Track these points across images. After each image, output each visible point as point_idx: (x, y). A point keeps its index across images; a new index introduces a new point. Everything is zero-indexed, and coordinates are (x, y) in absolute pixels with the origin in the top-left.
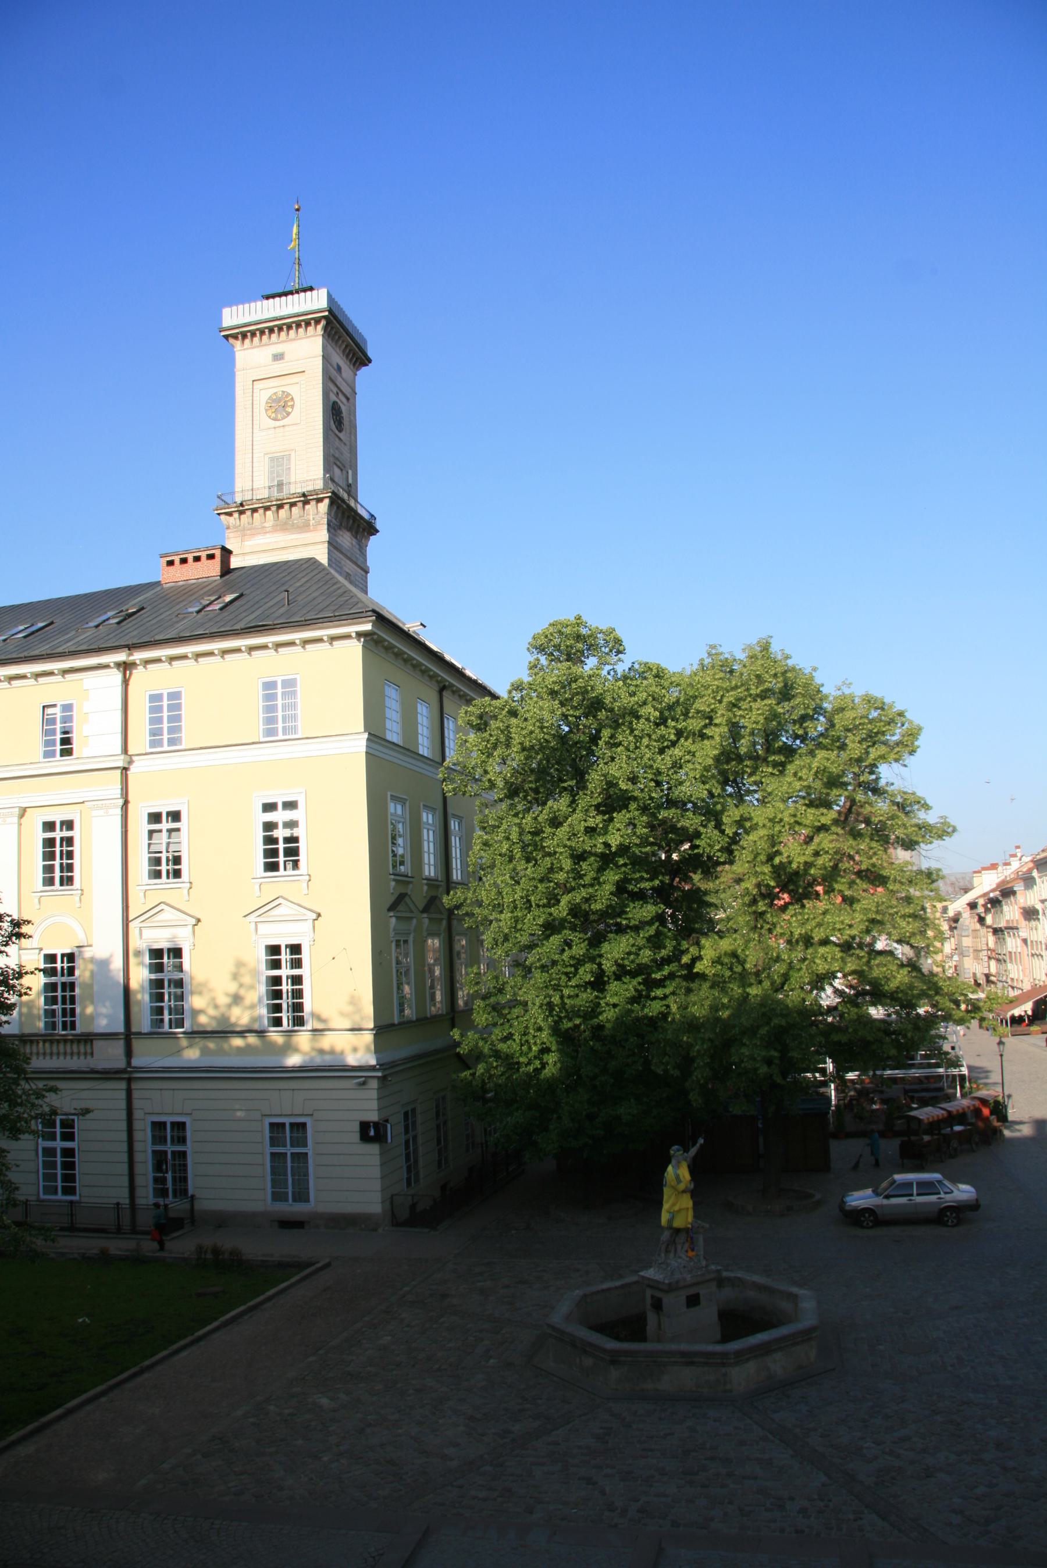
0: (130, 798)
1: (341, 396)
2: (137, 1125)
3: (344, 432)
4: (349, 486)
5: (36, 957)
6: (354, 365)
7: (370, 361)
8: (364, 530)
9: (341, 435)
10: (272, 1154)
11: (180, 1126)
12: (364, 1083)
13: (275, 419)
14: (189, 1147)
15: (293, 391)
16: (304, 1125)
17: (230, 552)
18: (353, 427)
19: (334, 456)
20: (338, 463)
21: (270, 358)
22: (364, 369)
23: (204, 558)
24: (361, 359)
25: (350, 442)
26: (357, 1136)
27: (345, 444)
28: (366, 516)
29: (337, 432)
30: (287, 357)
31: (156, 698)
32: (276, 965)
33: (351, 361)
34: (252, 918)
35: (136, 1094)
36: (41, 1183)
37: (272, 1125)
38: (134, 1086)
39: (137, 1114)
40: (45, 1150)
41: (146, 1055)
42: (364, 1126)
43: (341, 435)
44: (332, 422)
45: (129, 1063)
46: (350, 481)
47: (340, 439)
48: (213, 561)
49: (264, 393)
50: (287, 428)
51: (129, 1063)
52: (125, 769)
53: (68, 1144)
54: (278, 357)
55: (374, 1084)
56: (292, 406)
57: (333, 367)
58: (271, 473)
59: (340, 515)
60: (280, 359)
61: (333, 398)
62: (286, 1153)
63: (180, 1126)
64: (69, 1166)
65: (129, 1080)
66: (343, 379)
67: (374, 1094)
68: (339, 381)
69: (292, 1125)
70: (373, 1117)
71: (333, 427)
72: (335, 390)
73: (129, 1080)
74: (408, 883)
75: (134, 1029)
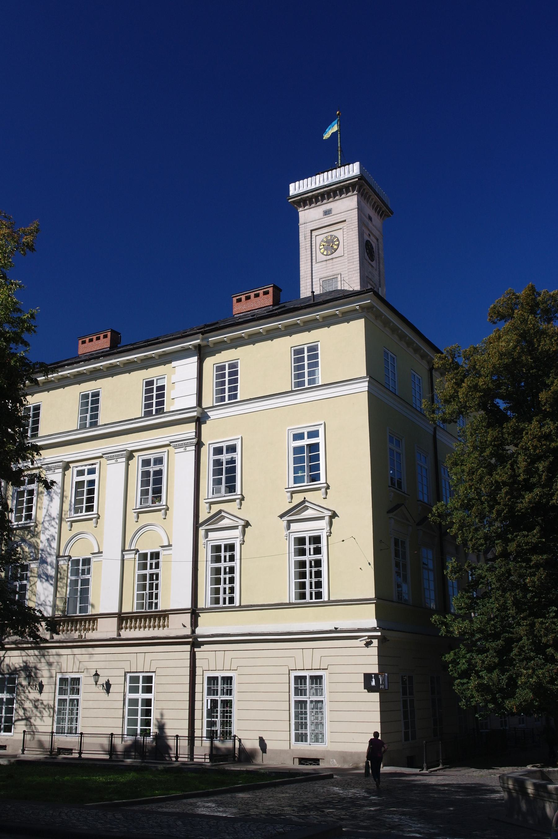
0: (203, 440)
2: (198, 680)
3: (374, 262)
5: (133, 556)
9: (372, 263)
11: (228, 680)
14: (235, 698)
15: (339, 234)
17: (280, 290)
20: (371, 282)
21: (322, 214)
23: (261, 295)
25: (379, 268)
26: (362, 685)
29: (370, 261)
30: (333, 213)
31: (221, 368)
32: (302, 552)
34: (286, 518)
35: (198, 655)
39: (199, 671)
40: (130, 700)
42: (368, 677)
43: (373, 263)
44: (366, 254)
45: (193, 632)
47: (372, 266)
48: (268, 295)
49: (320, 238)
50: (335, 260)
51: (193, 632)
53: (147, 696)
54: (327, 213)
55: (375, 642)
60: (329, 214)
61: (366, 238)
62: (306, 701)
63: (228, 680)
66: (373, 225)
67: (376, 650)
69: (311, 677)
70: (375, 670)
71: (367, 257)
72: (368, 232)
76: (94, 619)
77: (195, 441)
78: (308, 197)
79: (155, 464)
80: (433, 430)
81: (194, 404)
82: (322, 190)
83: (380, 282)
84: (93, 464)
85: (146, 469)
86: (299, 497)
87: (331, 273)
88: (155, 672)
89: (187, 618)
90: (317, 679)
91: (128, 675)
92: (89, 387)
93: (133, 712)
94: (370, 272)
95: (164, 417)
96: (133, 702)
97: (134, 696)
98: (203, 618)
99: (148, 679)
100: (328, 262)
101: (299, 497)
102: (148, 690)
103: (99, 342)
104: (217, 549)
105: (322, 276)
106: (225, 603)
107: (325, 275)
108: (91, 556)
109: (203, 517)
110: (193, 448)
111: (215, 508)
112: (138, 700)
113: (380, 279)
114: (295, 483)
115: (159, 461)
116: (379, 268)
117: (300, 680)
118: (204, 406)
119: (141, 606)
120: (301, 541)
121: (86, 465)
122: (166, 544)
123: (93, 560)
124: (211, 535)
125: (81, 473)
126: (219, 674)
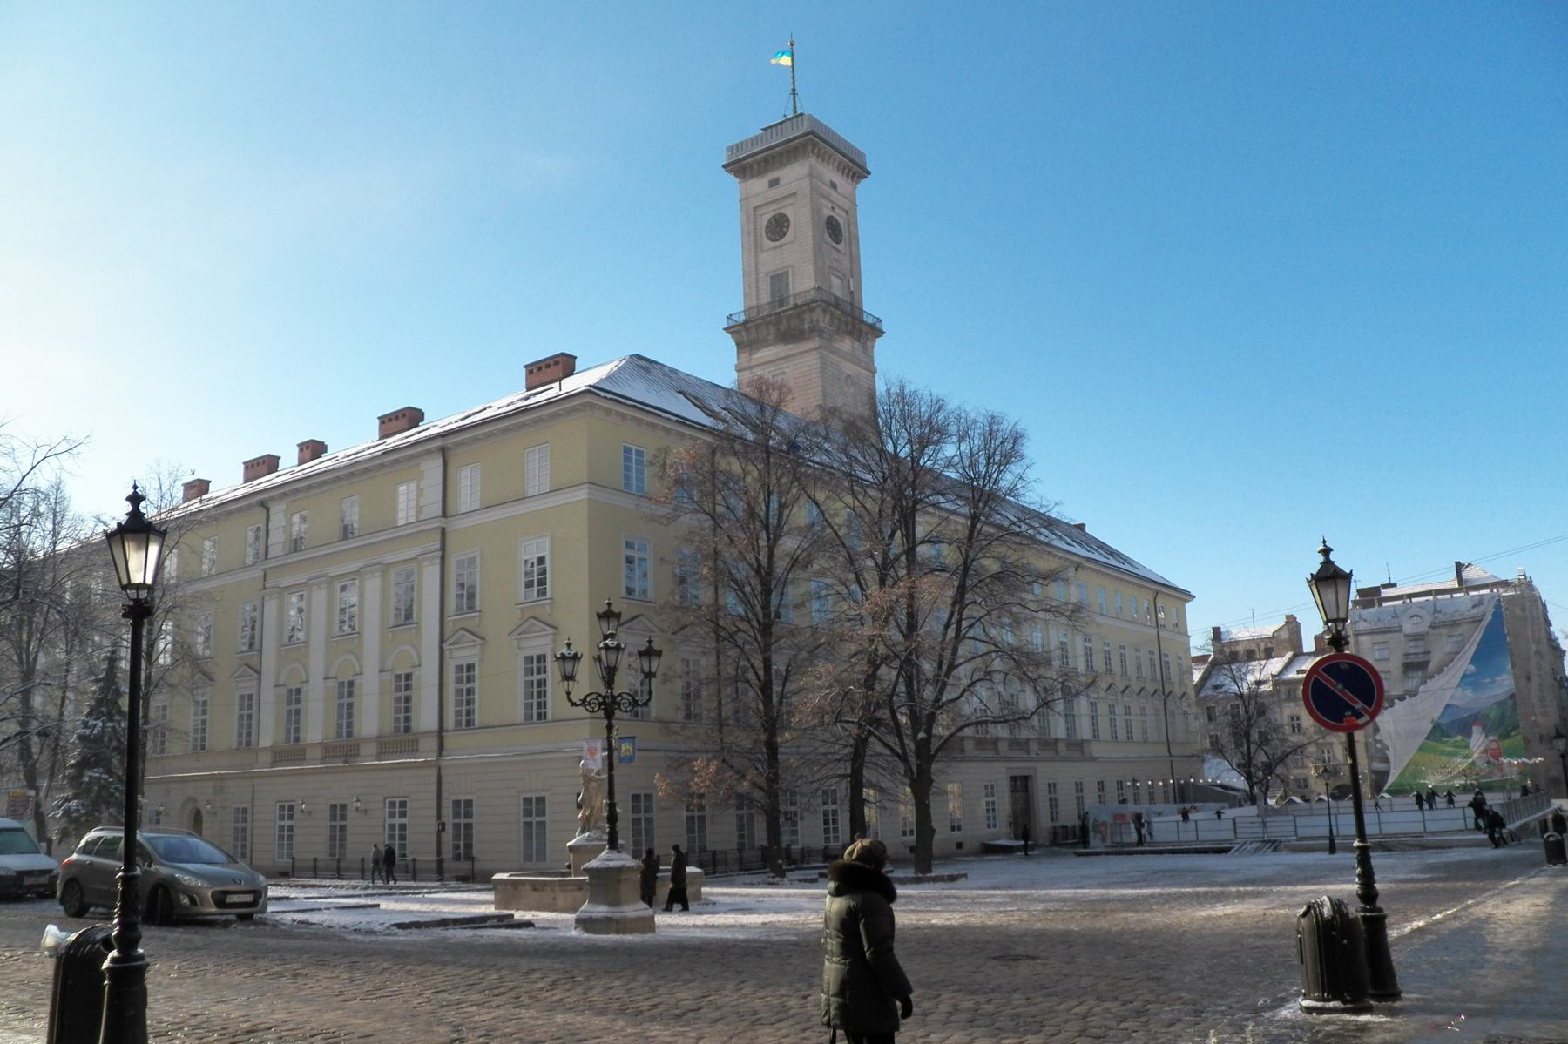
1: (837, 209)
4: (852, 293)
7: (869, 173)
8: (867, 334)
13: (774, 240)
14: (474, 820)
15: (788, 212)
18: (854, 239)
20: (836, 273)
22: (863, 182)
25: (850, 252)
29: (834, 244)
30: (781, 183)
34: (515, 636)
39: (445, 795)
43: (840, 247)
47: (838, 250)
53: (403, 821)
54: (774, 183)
56: (788, 227)
57: (826, 185)
58: (772, 290)
61: (827, 212)
72: (830, 205)
77: (439, 554)
91: (387, 801)
96: (392, 827)
99: (403, 804)
102: (403, 815)
104: (459, 668)
110: (438, 561)
115: (409, 575)
116: (850, 252)
117: (528, 801)
120: (529, 659)
124: (457, 653)
126: (534, 795)
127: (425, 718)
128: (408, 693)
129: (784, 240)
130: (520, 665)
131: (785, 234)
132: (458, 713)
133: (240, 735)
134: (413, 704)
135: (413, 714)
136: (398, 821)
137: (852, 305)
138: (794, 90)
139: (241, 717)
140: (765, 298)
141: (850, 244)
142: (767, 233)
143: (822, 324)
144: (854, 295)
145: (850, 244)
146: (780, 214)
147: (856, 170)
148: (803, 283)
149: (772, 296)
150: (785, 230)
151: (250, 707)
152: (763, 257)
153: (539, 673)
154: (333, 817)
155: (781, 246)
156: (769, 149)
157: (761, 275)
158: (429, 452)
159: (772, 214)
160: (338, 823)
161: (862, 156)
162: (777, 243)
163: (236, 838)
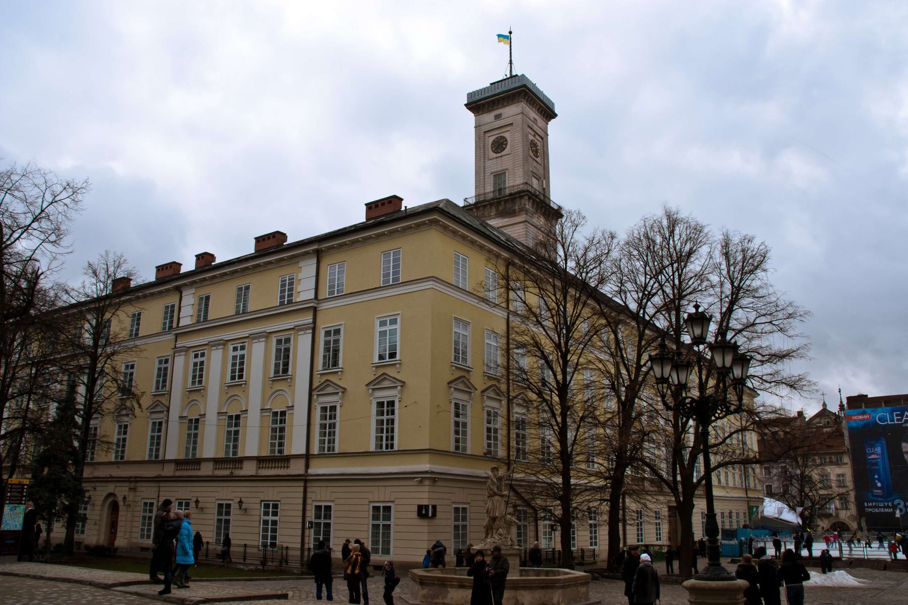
1: (537, 136)
2: (308, 507)
3: (539, 158)
4: (544, 189)
6: (546, 119)
7: (556, 115)
9: (536, 159)
10: (373, 525)
11: (328, 508)
12: (421, 482)
16: (389, 507)
19: (532, 171)
23: (386, 204)
24: (550, 114)
25: (544, 163)
26: (416, 514)
27: (540, 165)
28: (556, 207)
29: (534, 158)
33: (544, 116)
35: (309, 490)
36: (261, 540)
37: (374, 507)
38: (308, 485)
39: (309, 501)
40: (264, 521)
41: (318, 468)
42: (420, 507)
43: (538, 159)
45: (306, 471)
46: (544, 186)
47: (536, 161)
48: (391, 204)
50: (503, 158)
51: (306, 471)
52: (315, 310)
53: (275, 518)
54: (498, 117)
56: (506, 145)
58: (495, 184)
59: (535, 206)
61: (531, 137)
63: (328, 508)
64: (274, 531)
65: (306, 481)
68: (535, 128)
69: (384, 507)
70: (425, 502)
71: (532, 155)
72: (533, 133)
73: (306, 481)
74: (469, 371)
75: (311, 453)
76: (241, 460)
78: (482, 104)
79: (285, 343)
80: (506, 314)
81: (312, 296)
82: (493, 98)
83: (544, 175)
84: (243, 343)
85: (328, 338)
86: (381, 372)
87: (500, 169)
88: (279, 501)
89: (302, 462)
90: (388, 509)
92: (242, 282)
93: (265, 530)
94: (535, 167)
95: (293, 306)
96: (266, 522)
97: (266, 518)
98: (313, 462)
99: (275, 506)
100: (498, 159)
101: (381, 372)
102: (275, 514)
103: (269, 241)
105: (493, 171)
106: (387, 448)
107: (496, 170)
108: (240, 413)
109: (316, 384)
110: (311, 331)
111: (324, 378)
112: (269, 521)
113: (544, 173)
114: (379, 360)
115: (288, 340)
116: (544, 163)
117: (376, 509)
118: (320, 297)
119: (273, 451)
121: (239, 343)
122: (290, 405)
123: (242, 416)
125: (235, 349)
127: (296, 445)
128: (282, 425)
129: (504, 153)
130: (374, 409)
131: (504, 149)
132: (322, 442)
133: (151, 450)
134: (286, 433)
135: (286, 441)
136: (270, 518)
137: (544, 196)
138: (511, 61)
139: (152, 437)
140: (489, 188)
141: (544, 158)
142: (492, 148)
143: (527, 206)
144: (546, 191)
145: (544, 158)
146: (501, 136)
147: (548, 113)
148: (515, 181)
149: (495, 187)
150: (504, 146)
151: (159, 430)
152: (488, 163)
153: (330, 419)
154: (220, 513)
155: (502, 156)
156: (495, 95)
157: (487, 174)
158: (307, 253)
159: (496, 136)
160: (224, 517)
161: (553, 104)
162: (499, 155)
163: (143, 524)
